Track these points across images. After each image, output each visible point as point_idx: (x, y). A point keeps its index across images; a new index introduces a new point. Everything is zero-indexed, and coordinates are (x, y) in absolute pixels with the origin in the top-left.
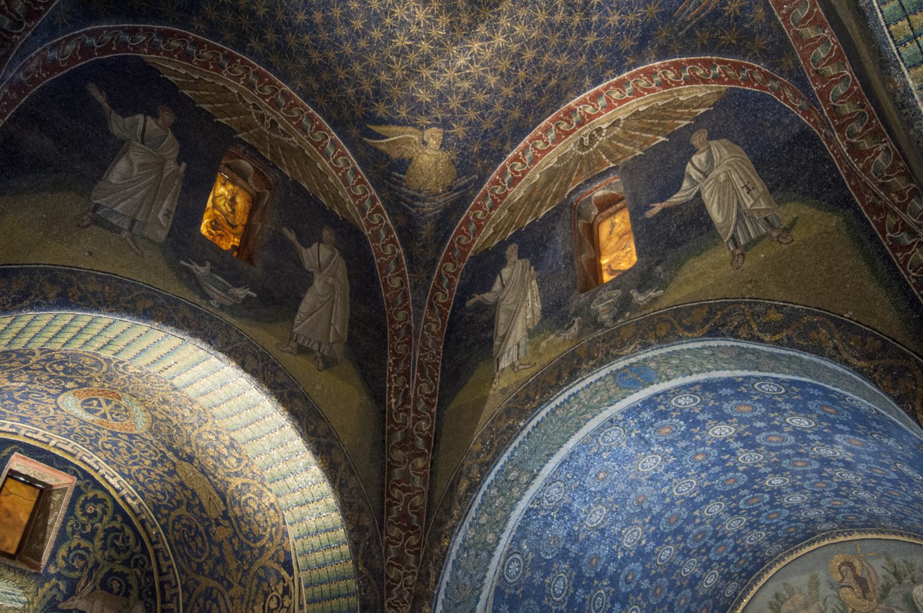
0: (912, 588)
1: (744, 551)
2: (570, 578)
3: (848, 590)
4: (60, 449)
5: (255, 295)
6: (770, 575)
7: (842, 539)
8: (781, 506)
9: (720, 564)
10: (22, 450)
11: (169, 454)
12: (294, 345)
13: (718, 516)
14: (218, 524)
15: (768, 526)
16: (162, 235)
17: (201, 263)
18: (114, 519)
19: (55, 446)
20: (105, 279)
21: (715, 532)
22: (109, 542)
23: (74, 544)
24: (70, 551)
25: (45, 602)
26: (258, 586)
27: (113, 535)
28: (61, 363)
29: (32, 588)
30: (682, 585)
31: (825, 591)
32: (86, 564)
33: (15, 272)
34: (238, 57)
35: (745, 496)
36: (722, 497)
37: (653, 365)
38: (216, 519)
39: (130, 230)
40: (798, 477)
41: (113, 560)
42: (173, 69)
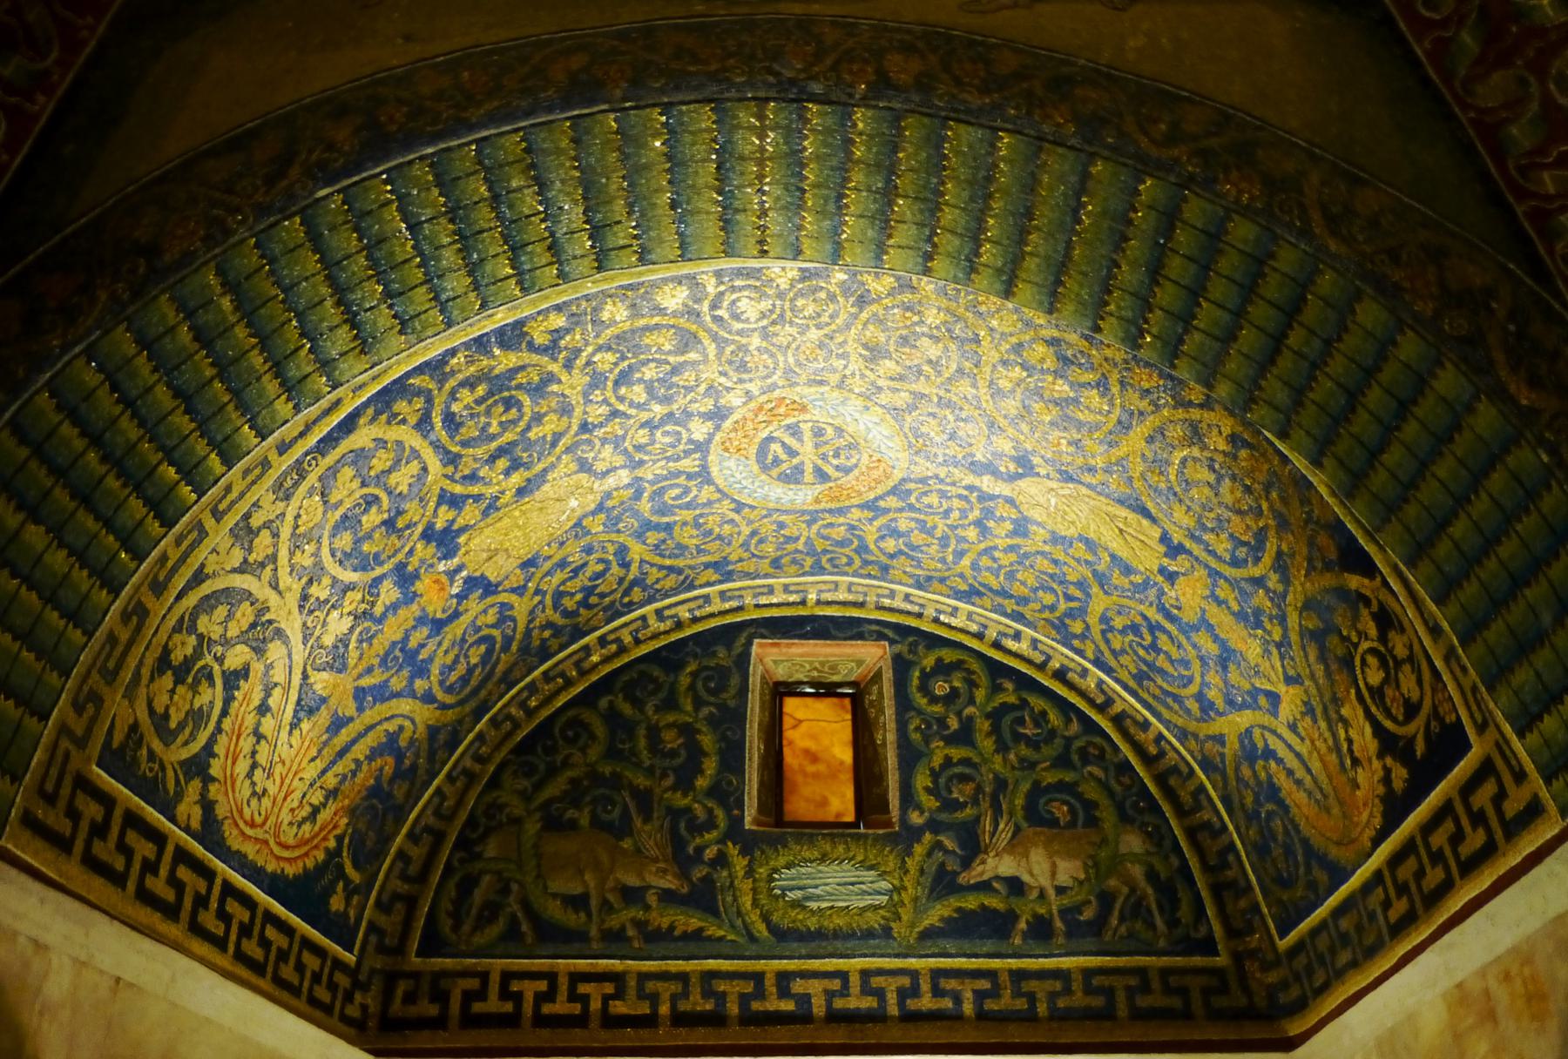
4: (829, 603)
10: (763, 631)
11: (987, 483)
14: (1171, 577)
18: (996, 689)
19: (819, 602)
22: (1007, 735)
23: (937, 761)
24: (935, 775)
25: (927, 881)
26: (1322, 658)
27: (1007, 720)
28: (623, 379)
29: (892, 863)
32: (979, 789)
38: (1162, 570)
41: (1032, 765)
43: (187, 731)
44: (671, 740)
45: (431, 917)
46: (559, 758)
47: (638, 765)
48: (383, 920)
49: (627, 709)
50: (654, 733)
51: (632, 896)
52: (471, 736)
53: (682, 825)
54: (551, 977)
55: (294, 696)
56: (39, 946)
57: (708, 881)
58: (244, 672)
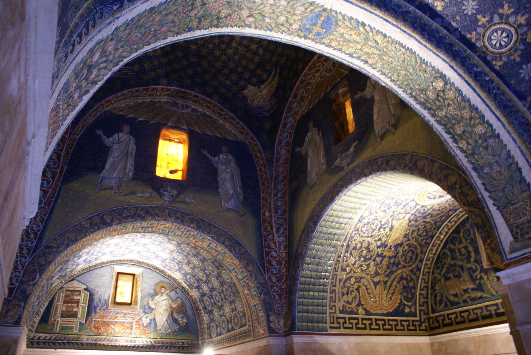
5: (357, 142)
12: (378, 140)
16: (324, 167)
17: (336, 160)
20: (318, 205)
33: (304, 228)
34: (302, 79)
37: (296, 26)
39: (318, 178)
42: (304, 109)
43: (354, 301)
44: (463, 251)
45: (431, 305)
46: (443, 263)
47: (458, 260)
48: (423, 308)
49: (452, 246)
50: (459, 250)
51: (466, 291)
52: (423, 266)
53: (471, 271)
54: (455, 313)
55: (372, 284)
56: (340, 343)
57: (480, 283)
58: (359, 286)
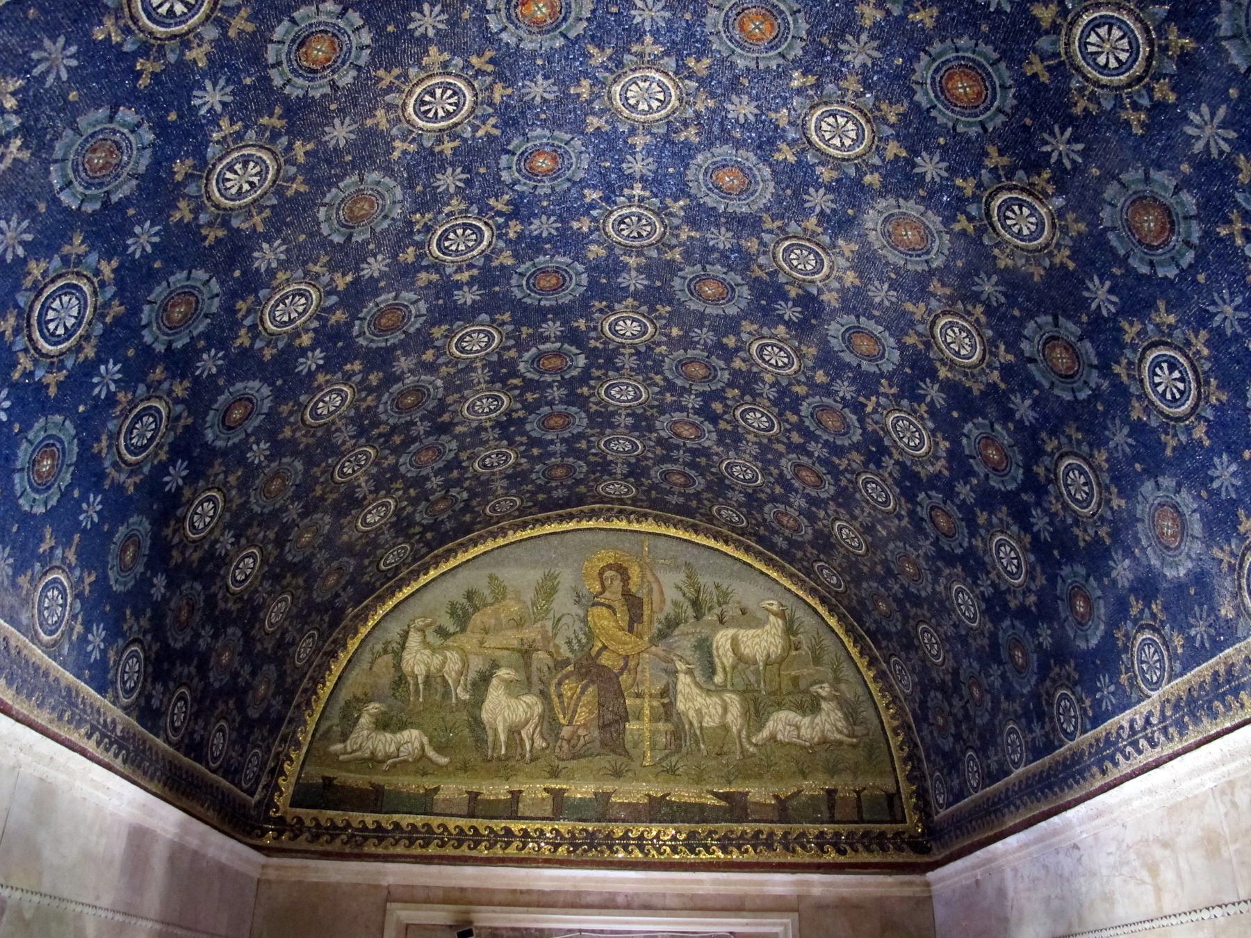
0: (715, 631)
1: (458, 483)
2: (99, 314)
3: (605, 611)
6: (469, 555)
7: (623, 525)
8: (582, 402)
9: (406, 490)
13: (470, 368)
15: (533, 442)
21: (442, 407)
30: (322, 499)
31: (563, 603)
35: (547, 339)
36: (507, 317)
40: (675, 332)
